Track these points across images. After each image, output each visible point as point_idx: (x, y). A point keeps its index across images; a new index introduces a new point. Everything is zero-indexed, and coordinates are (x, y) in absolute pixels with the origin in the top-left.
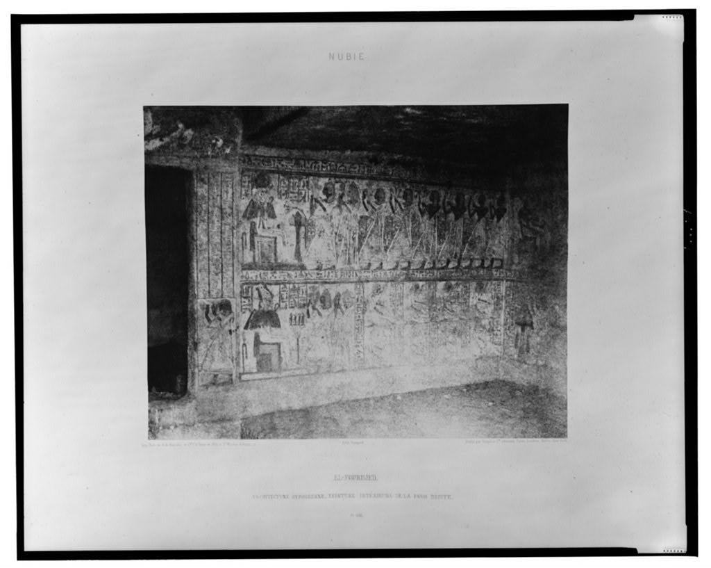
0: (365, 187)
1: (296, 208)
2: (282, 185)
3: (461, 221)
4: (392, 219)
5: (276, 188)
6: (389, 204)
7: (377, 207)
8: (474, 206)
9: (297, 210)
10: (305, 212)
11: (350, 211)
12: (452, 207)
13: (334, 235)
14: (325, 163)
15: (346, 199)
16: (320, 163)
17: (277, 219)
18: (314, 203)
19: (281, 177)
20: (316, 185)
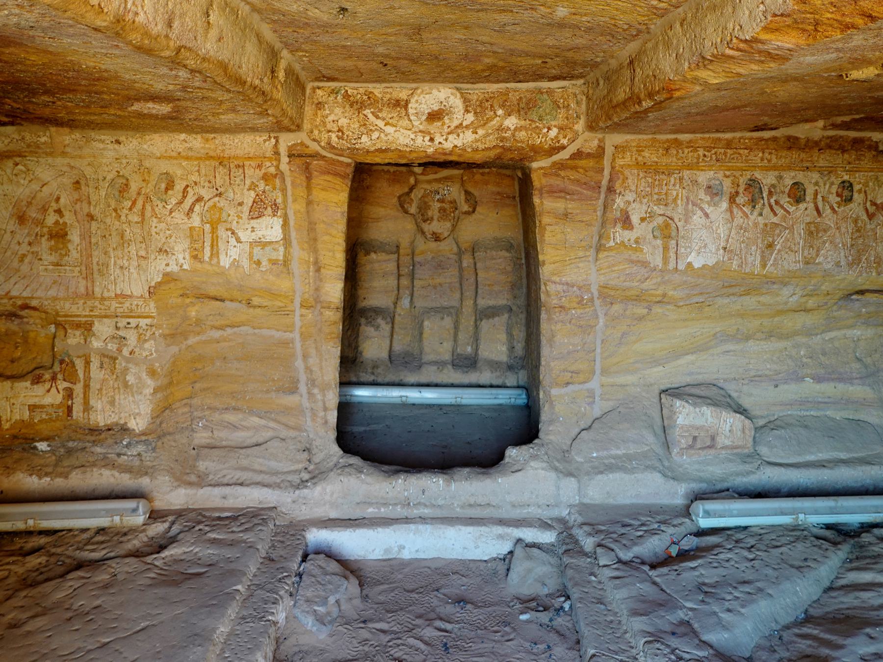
0: (774, 182)
2: (643, 184)
5: (633, 188)
6: (812, 205)
7: (792, 209)
9: (665, 218)
10: (676, 220)
13: (722, 251)
14: (708, 151)
15: (740, 200)
16: (701, 152)
18: (690, 206)
19: (641, 175)
20: (695, 182)
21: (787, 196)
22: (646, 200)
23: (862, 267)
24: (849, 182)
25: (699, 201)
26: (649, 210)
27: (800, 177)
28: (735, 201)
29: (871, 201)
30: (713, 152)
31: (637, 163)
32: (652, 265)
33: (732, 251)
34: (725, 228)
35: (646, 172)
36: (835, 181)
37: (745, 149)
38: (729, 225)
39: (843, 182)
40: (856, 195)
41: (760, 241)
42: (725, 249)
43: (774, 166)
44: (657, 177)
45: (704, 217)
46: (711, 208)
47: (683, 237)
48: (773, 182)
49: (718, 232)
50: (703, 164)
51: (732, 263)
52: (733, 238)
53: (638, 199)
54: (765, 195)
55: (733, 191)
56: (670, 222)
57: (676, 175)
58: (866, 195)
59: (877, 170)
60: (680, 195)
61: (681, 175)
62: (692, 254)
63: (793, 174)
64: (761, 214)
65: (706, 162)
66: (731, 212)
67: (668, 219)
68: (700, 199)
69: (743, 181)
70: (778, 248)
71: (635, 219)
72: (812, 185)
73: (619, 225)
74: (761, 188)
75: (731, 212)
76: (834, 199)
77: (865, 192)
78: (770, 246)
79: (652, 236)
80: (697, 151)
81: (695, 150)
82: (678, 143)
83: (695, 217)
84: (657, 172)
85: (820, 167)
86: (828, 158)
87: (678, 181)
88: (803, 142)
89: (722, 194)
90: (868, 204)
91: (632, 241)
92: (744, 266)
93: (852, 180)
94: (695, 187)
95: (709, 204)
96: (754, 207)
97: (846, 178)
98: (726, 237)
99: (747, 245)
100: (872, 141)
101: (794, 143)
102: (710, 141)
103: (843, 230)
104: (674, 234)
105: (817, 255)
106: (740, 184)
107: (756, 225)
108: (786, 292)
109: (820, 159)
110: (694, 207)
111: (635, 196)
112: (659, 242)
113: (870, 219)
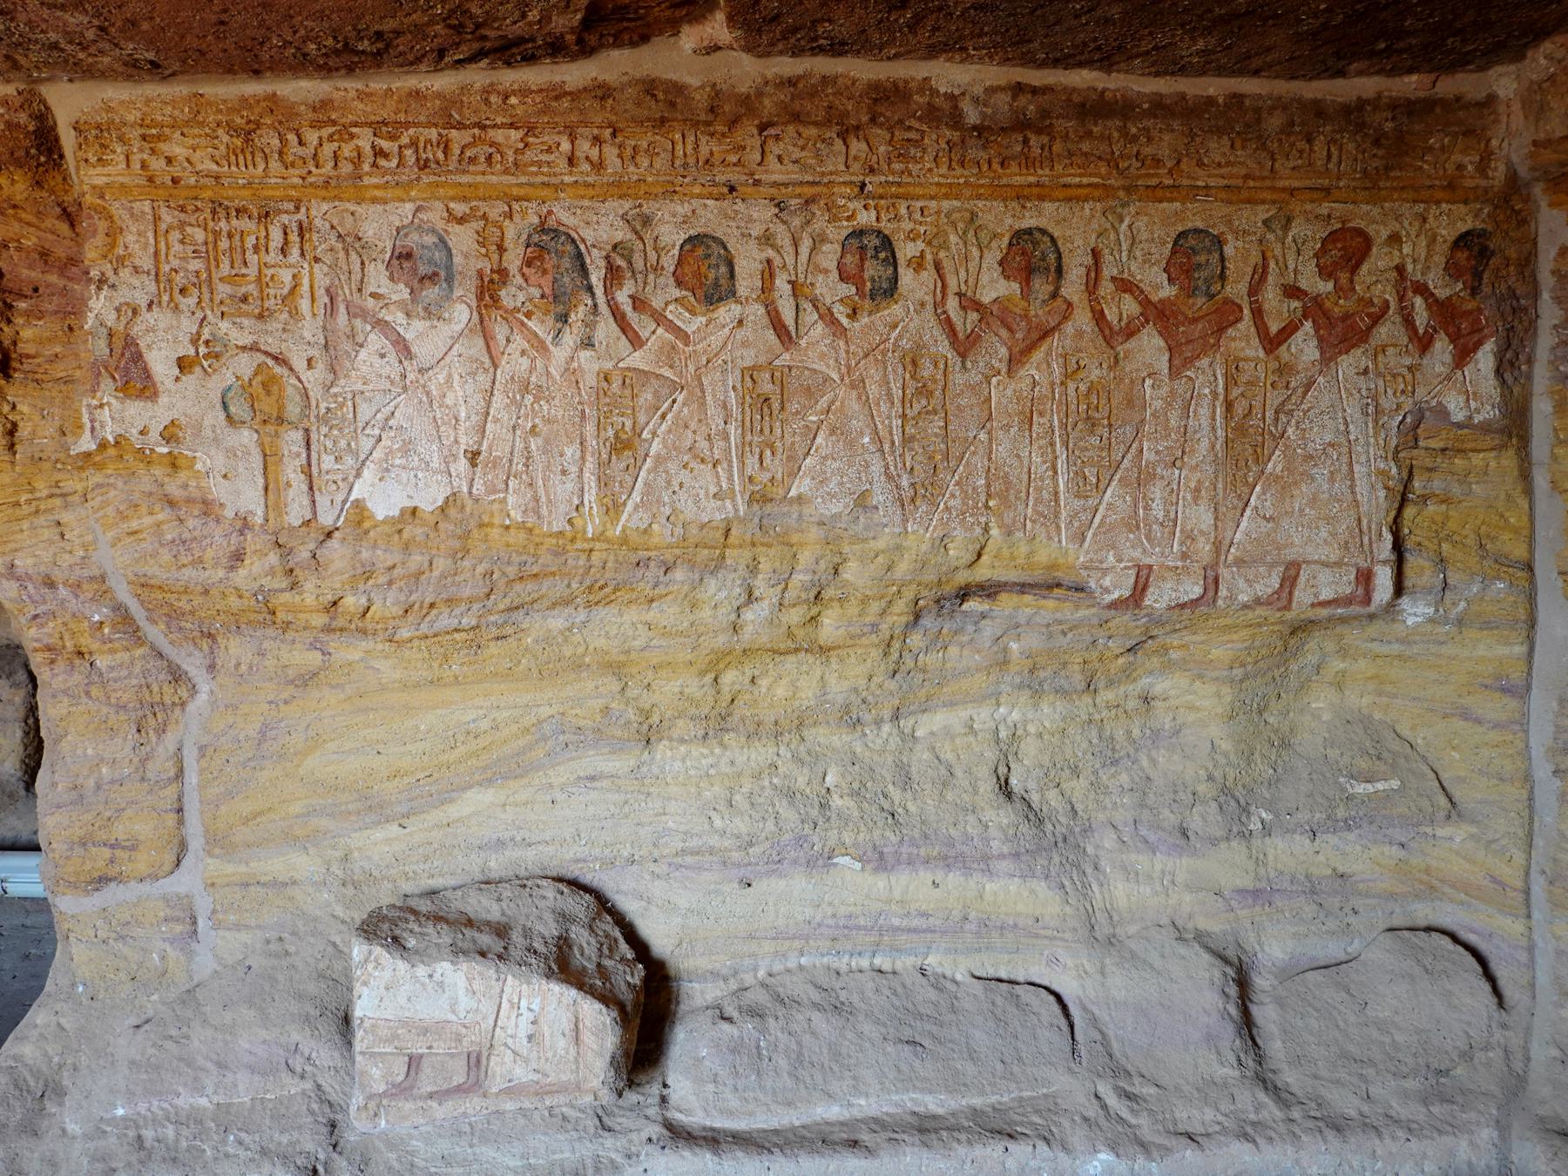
0: (622, 234)
1: (254, 348)
2: (177, 247)
3: (1207, 376)
4: (780, 378)
5: (147, 263)
7: (692, 324)
8: (1292, 291)
9: (261, 358)
10: (299, 364)
11: (542, 347)
12: (1146, 302)
13: (462, 464)
15: (510, 296)
16: (365, 140)
17: (163, 399)
19: (168, 218)
20: (351, 241)
21: (671, 281)
22: (191, 301)
23: (947, 508)
24: (879, 232)
25: (371, 302)
26: (206, 335)
27: (710, 216)
28: (496, 300)
29: (960, 295)
30: (405, 140)
31: (151, 179)
32: (229, 513)
33: (495, 463)
34: (470, 388)
35: (183, 209)
36: (831, 232)
37: (512, 126)
38: (481, 378)
39: (859, 233)
40: (906, 277)
41: (590, 429)
42: (473, 457)
43: (617, 184)
44: (223, 224)
45: (392, 357)
46: (419, 325)
47: (323, 420)
48: (619, 236)
49: (449, 401)
50: (375, 180)
51: (504, 501)
52: (496, 421)
53: (165, 298)
54: (596, 278)
55: (487, 267)
56: (278, 370)
57: (285, 218)
58: (941, 277)
59: (967, 192)
60: (306, 282)
61: (302, 215)
62: (366, 473)
63: (682, 209)
64: (588, 343)
65: (386, 172)
66: (488, 338)
67: (270, 362)
68: (373, 295)
69: (514, 232)
70: (656, 447)
71: (160, 363)
72: (753, 244)
73: (107, 384)
74: (579, 255)
75: (488, 338)
76: (831, 289)
77: (938, 266)
78: (623, 445)
79: (222, 416)
80: (352, 136)
81: (345, 133)
82: (278, 111)
83: (363, 354)
84: (217, 208)
85: (775, 184)
86: (797, 154)
87: (294, 237)
88: (701, 99)
89: (449, 280)
90: (952, 304)
91: (154, 435)
92: (544, 511)
93: (887, 227)
94: (353, 256)
95: (401, 304)
96: (563, 318)
97: (866, 218)
98: (474, 418)
99: (547, 441)
100: (934, 92)
101: (672, 104)
102: (391, 104)
103: (873, 390)
104: (293, 410)
105: (793, 474)
106: (508, 243)
107: (572, 374)
108: (720, 592)
109: (771, 159)
110: (358, 323)
111: (152, 287)
112: (246, 437)
113: (963, 356)
